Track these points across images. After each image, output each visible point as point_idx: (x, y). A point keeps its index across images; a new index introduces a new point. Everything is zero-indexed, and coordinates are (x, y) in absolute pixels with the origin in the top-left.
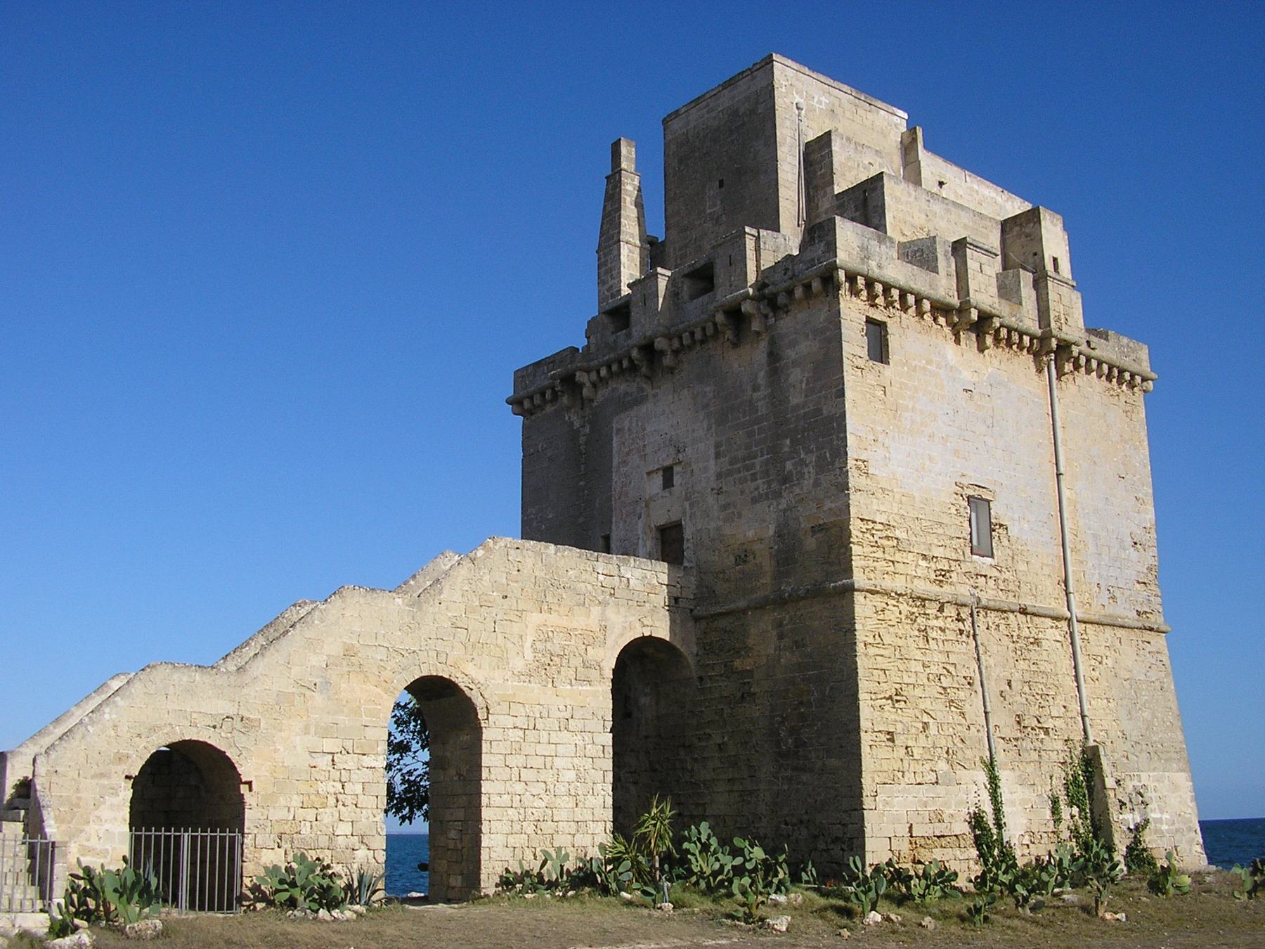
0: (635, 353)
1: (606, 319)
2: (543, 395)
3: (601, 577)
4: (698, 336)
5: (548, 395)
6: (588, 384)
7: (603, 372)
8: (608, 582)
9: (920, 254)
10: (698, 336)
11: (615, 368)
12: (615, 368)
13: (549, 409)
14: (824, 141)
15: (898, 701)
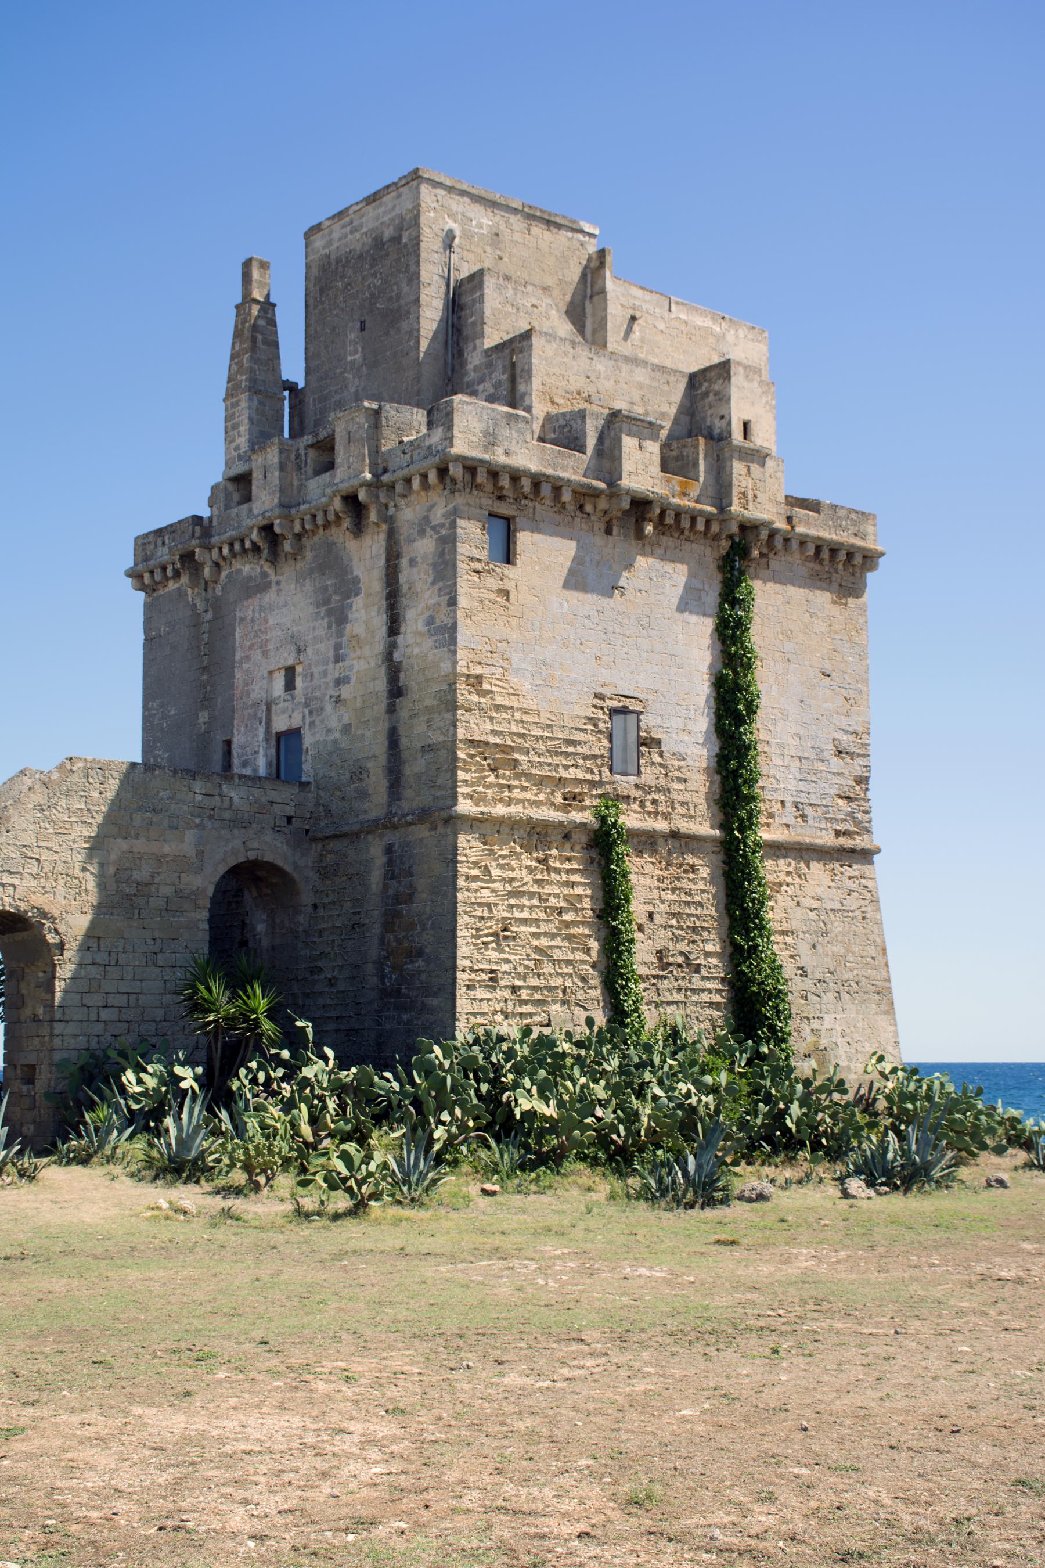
0: (255, 535)
1: (231, 487)
2: (164, 569)
3: (199, 798)
4: (320, 521)
5: (169, 572)
6: (209, 563)
7: (226, 551)
8: (208, 802)
9: (564, 433)
10: (320, 521)
11: (237, 546)
12: (237, 546)
13: (172, 586)
14: (476, 279)
15: (506, 938)
